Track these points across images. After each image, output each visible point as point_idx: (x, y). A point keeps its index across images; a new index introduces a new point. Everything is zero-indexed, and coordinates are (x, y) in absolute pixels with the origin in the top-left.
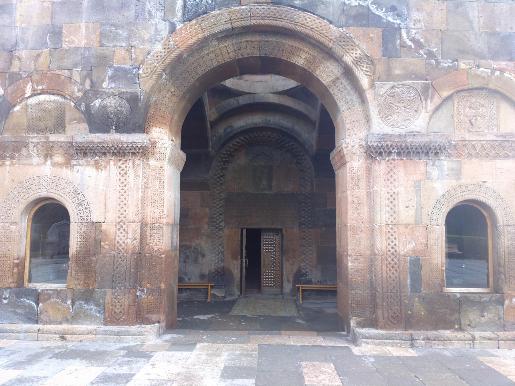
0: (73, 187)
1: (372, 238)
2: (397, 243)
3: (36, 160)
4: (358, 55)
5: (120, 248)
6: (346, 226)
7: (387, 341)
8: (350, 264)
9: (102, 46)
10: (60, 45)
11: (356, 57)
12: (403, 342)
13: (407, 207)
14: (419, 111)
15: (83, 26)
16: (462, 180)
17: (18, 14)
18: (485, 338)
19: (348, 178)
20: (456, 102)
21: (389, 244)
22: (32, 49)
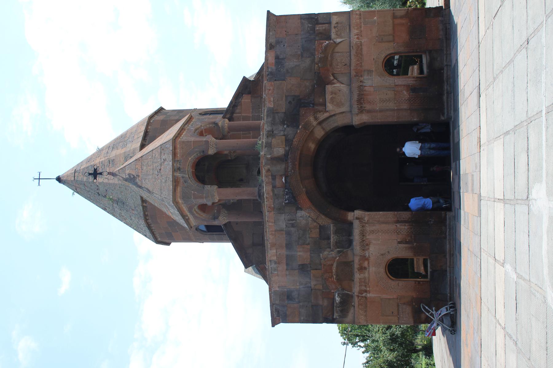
0: (380, 256)
1: (402, 110)
2: (404, 99)
3: (366, 275)
4: (313, 119)
5: (410, 232)
6: (396, 121)
7: (449, 104)
8: (415, 120)
9: (309, 244)
10: (309, 265)
11: (314, 120)
12: (449, 97)
13: (386, 94)
14: (340, 90)
15: (299, 253)
16: (373, 69)
17: (292, 287)
18: (446, 60)
19: (372, 121)
20: (335, 72)
21: (405, 102)
22: (310, 279)
